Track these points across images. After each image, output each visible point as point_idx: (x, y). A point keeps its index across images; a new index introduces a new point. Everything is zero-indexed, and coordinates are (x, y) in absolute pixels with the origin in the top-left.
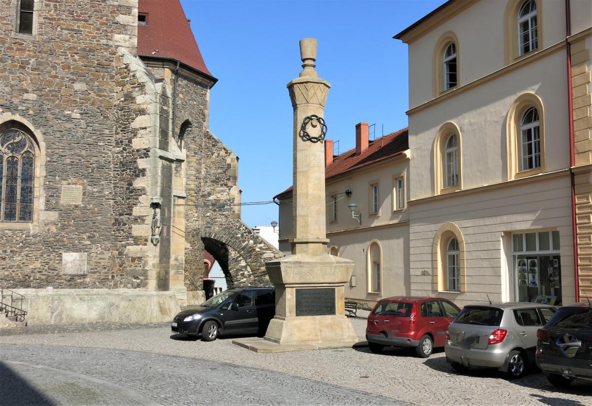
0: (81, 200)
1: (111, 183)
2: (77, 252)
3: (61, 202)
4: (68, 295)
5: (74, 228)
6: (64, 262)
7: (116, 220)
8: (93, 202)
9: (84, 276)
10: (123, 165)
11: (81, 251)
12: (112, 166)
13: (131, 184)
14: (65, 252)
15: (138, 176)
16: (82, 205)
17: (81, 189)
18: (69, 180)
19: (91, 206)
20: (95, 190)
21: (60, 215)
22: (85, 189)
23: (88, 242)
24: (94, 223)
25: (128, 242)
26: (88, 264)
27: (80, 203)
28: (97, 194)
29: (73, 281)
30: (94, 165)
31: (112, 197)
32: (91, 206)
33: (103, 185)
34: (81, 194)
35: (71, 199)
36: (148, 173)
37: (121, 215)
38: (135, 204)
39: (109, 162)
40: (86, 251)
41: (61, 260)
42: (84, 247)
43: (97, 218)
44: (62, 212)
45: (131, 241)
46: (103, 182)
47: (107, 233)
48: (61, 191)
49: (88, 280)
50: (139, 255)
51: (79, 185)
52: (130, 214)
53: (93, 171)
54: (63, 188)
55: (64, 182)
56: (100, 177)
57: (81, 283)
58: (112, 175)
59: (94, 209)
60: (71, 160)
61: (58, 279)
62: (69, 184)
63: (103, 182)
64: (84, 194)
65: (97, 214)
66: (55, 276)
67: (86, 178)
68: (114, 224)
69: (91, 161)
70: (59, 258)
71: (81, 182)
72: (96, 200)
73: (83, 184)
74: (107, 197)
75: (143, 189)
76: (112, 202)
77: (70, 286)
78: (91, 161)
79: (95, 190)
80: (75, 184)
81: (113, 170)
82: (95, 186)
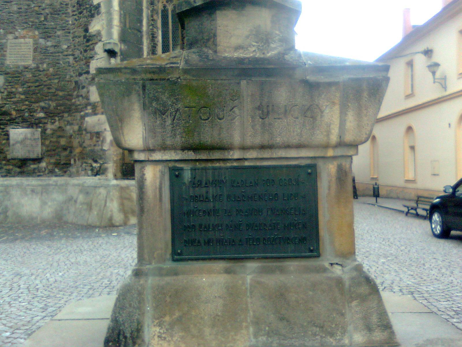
0: (31, 58)
1: (69, 33)
2: (28, 127)
3: (8, 62)
4: (18, 185)
5: (23, 97)
6: (12, 142)
7: (76, 82)
8: (47, 60)
9: (38, 160)
10: (80, 6)
11: (32, 127)
12: (70, 10)
13: (86, 30)
14: (13, 128)
15: (92, 16)
16: (34, 66)
17: (32, 44)
18: (16, 33)
19: (45, 66)
20: (49, 44)
21: (7, 81)
22: (36, 43)
23: (42, 115)
24: (49, 88)
25: (87, 111)
26: (42, 144)
27: (30, 62)
28: (52, 50)
29: (23, 166)
30: (47, 11)
31: (71, 53)
32: (45, 66)
33: (59, 36)
34: (32, 50)
35: (19, 58)
36: (103, 9)
37: (80, 75)
38: (91, 58)
39: (66, 5)
40: (40, 127)
41: (8, 139)
42: (37, 121)
43: (52, 81)
44: (8, 76)
45: (89, 110)
46: (59, 33)
47: (67, 102)
48: (6, 48)
49: (43, 164)
50: (97, 129)
51: (29, 38)
52: (88, 72)
53: (46, 19)
54: (9, 45)
55: (10, 37)
56: (54, 26)
57: (34, 169)
58: (71, 22)
59: (48, 70)
60: (18, 7)
61: (5, 165)
62: (16, 38)
63: (59, 33)
64: (35, 50)
65: (52, 77)
66: (3, 160)
67: (37, 28)
68: (74, 89)
69: (44, 5)
70: (6, 137)
71: (30, 34)
72: (51, 57)
73: (33, 37)
74: (66, 53)
75: (99, 33)
76: (71, 59)
77: (22, 174)
78: (44, 5)
79: (49, 44)
80: (24, 37)
81: (71, 14)
82: (50, 39)
